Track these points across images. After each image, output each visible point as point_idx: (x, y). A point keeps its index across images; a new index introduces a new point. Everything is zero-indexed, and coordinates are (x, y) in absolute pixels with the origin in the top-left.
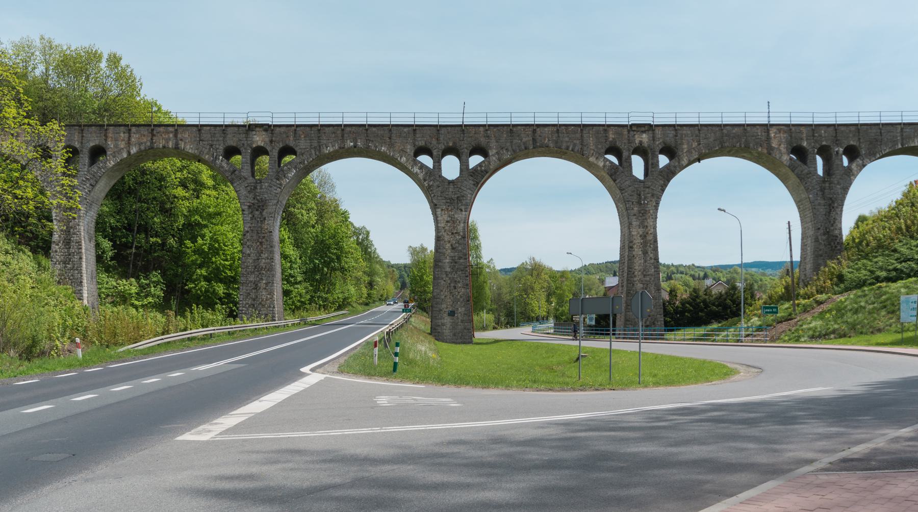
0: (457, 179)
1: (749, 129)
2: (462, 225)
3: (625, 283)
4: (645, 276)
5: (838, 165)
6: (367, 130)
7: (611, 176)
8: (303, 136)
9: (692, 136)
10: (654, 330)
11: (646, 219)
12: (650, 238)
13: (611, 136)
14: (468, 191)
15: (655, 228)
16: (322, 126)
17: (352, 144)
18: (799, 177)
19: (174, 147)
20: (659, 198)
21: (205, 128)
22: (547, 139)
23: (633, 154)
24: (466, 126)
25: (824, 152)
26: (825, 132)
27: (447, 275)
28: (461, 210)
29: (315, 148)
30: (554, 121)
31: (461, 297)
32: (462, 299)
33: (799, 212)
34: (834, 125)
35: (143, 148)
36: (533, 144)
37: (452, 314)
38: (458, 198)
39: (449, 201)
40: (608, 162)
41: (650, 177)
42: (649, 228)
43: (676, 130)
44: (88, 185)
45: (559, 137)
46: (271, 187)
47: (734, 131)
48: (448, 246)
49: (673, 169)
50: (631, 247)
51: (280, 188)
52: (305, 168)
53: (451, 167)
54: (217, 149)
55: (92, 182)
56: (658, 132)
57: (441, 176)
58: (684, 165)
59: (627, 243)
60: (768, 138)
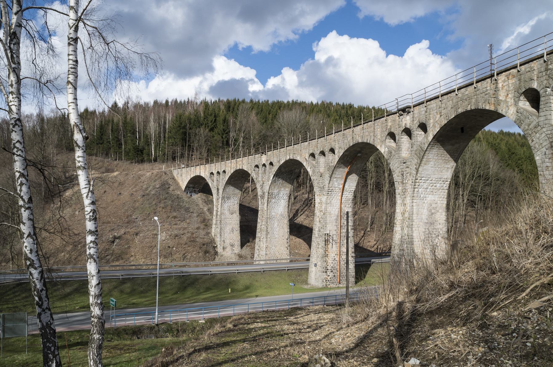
11: (405, 197)
42: (407, 205)
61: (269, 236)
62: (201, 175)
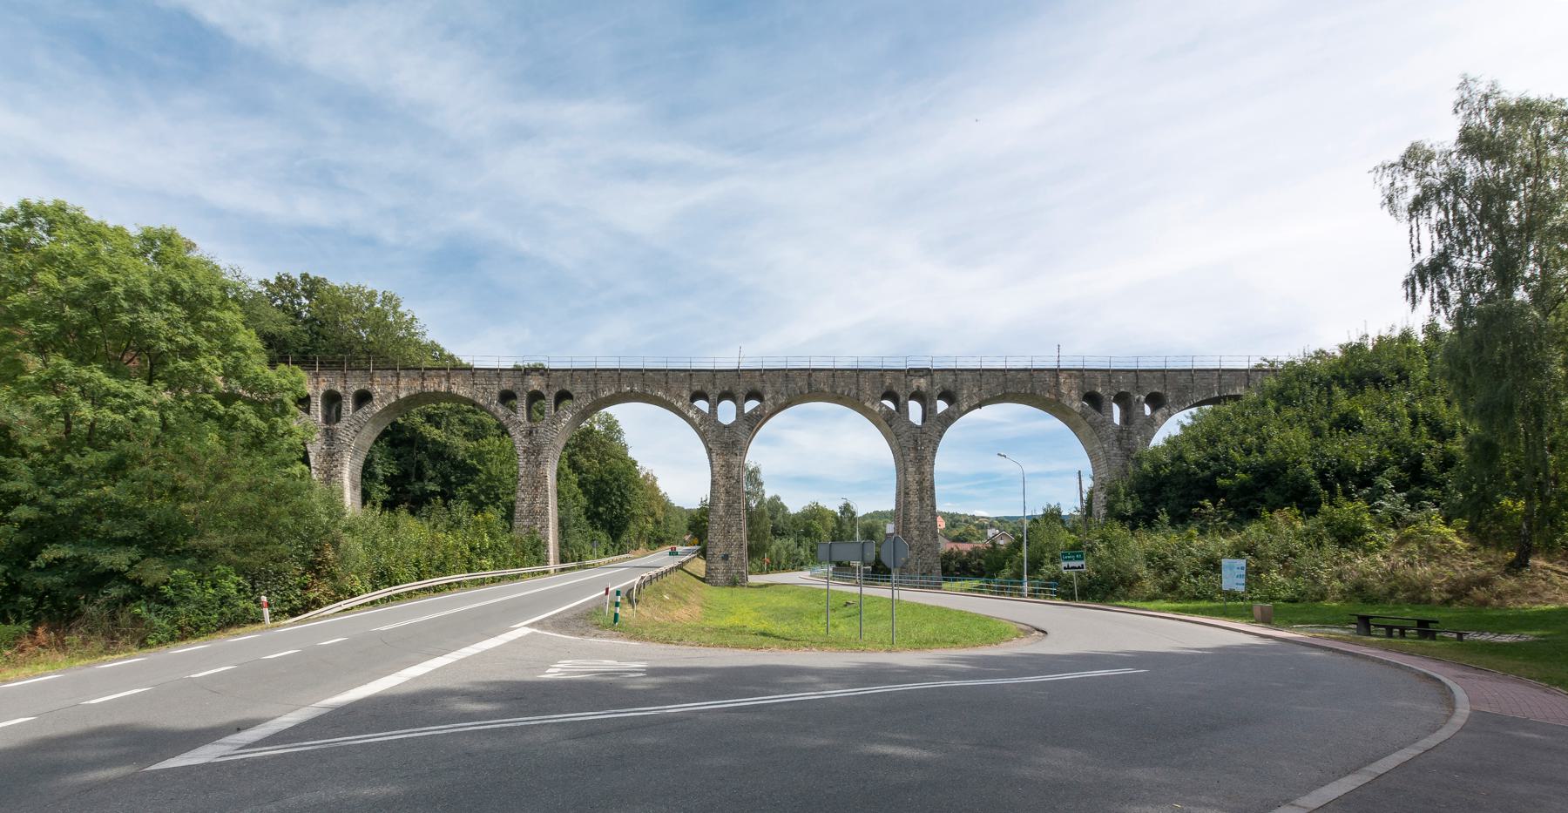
0: (732, 423)
1: (1035, 373)
3: (901, 530)
4: (921, 523)
5: (1138, 413)
6: (643, 374)
7: (887, 421)
9: (973, 381)
10: (931, 579)
11: (923, 465)
12: (927, 484)
13: (888, 381)
15: (932, 474)
16: (599, 370)
17: (629, 388)
18: (1091, 426)
20: (937, 444)
21: (479, 372)
23: (910, 399)
24: (742, 370)
25: (1122, 399)
26: (1124, 378)
29: (592, 392)
30: (830, 366)
33: (1092, 462)
34: (1135, 371)
35: (413, 392)
38: (733, 442)
40: (884, 408)
41: (927, 423)
43: (956, 375)
45: (834, 381)
47: (1019, 376)
48: (722, 490)
49: (952, 415)
50: (907, 494)
52: (582, 412)
53: (727, 412)
54: (491, 393)
55: (357, 427)
56: (937, 376)
57: (716, 421)
58: (964, 410)
59: (902, 488)
60: (1057, 384)
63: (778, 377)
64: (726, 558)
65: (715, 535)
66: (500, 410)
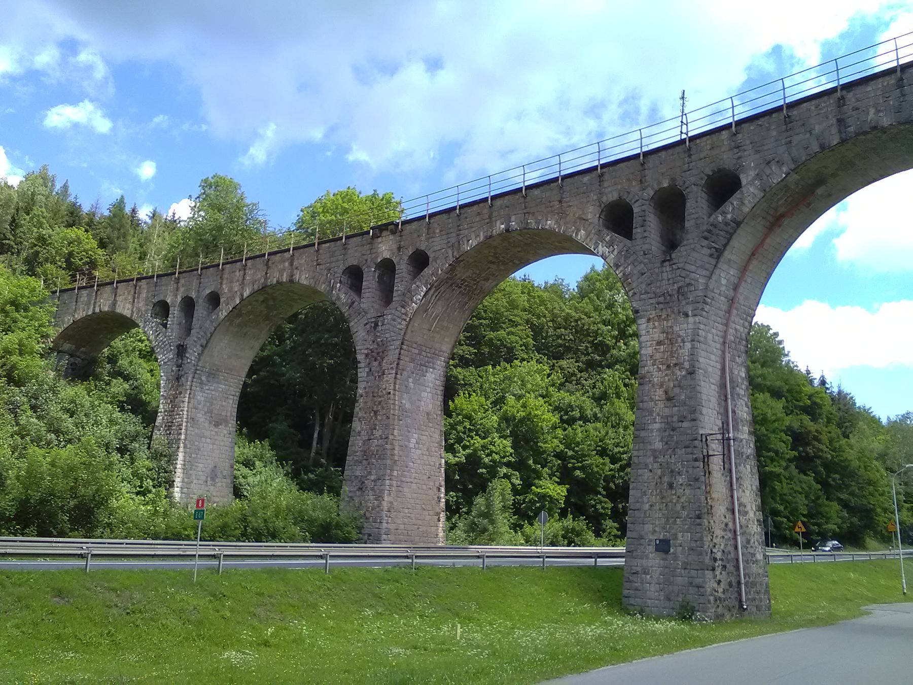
2: (688, 345)
8: (438, 231)
14: (700, 271)
17: (503, 226)
19: (288, 280)
22: (872, 111)
27: (655, 457)
28: (687, 315)
31: (683, 508)
32: (685, 513)
35: (256, 287)
36: (840, 132)
37: (663, 547)
38: (679, 288)
39: (661, 299)
44: (198, 346)
45: (903, 95)
46: (394, 320)
48: (660, 392)
51: (405, 320)
61: (395, 473)
62: (119, 310)
63: (768, 129)
64: (663, 547)
65: (645, 493)
66: (343, 296)
